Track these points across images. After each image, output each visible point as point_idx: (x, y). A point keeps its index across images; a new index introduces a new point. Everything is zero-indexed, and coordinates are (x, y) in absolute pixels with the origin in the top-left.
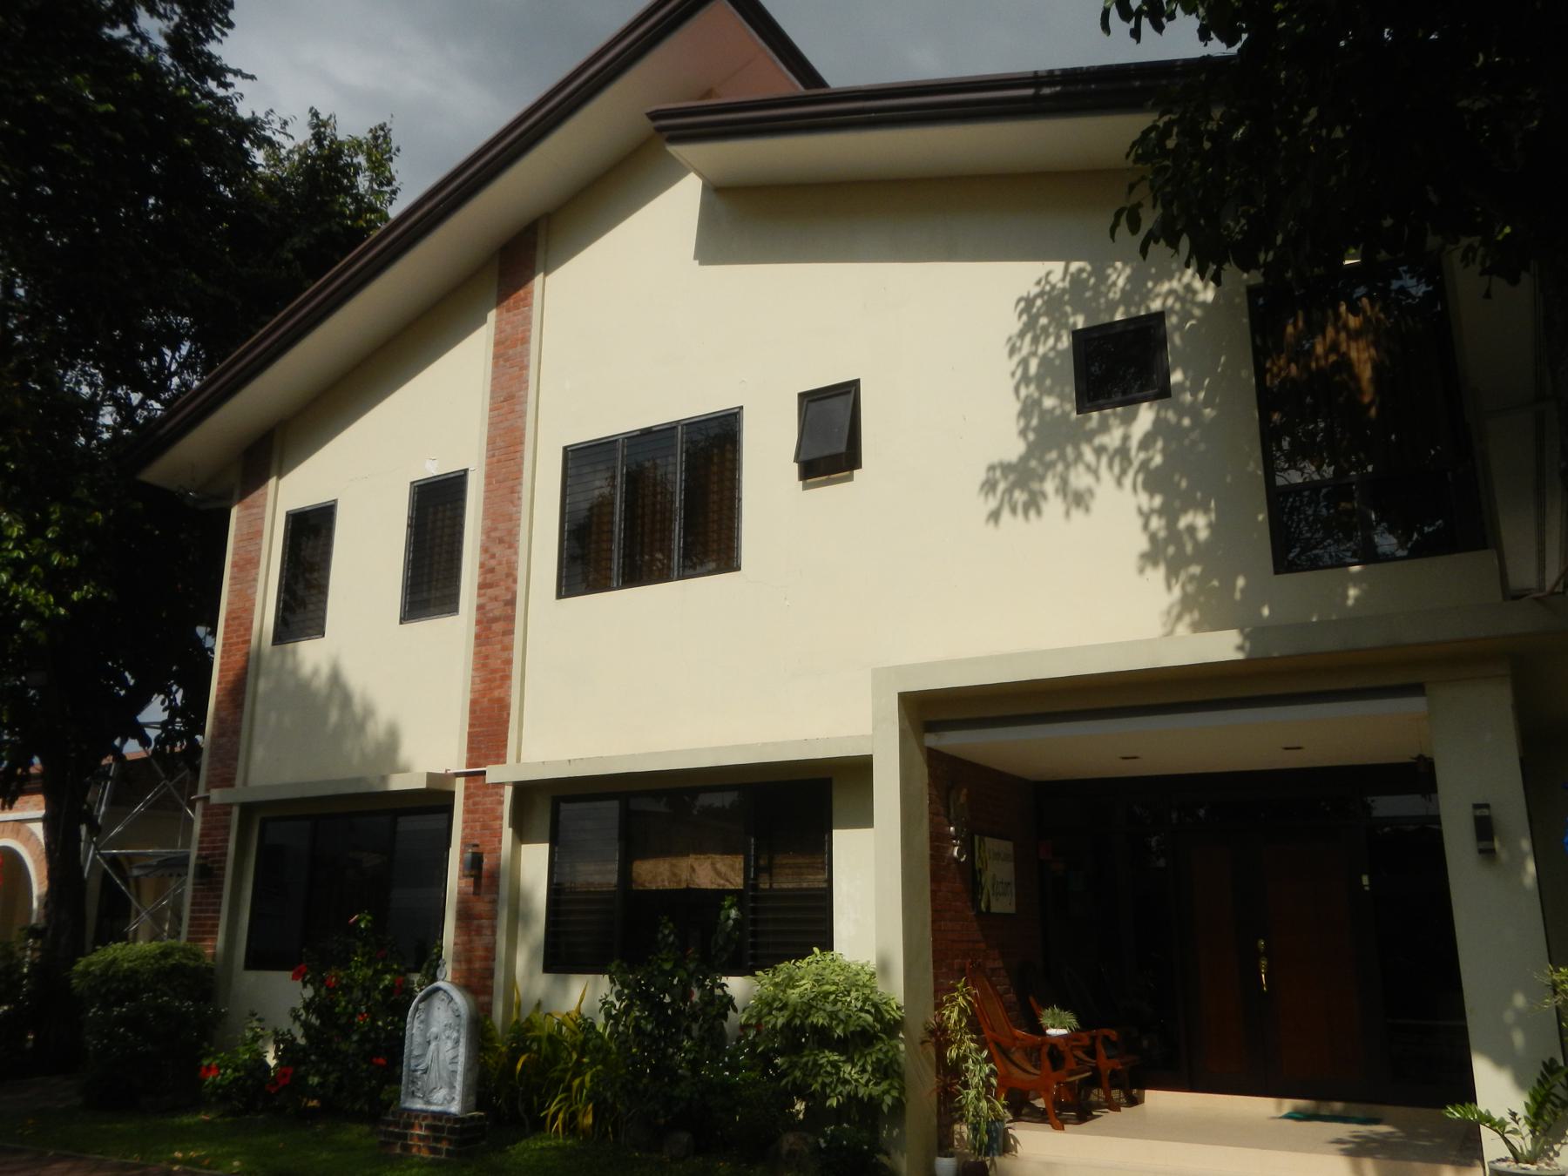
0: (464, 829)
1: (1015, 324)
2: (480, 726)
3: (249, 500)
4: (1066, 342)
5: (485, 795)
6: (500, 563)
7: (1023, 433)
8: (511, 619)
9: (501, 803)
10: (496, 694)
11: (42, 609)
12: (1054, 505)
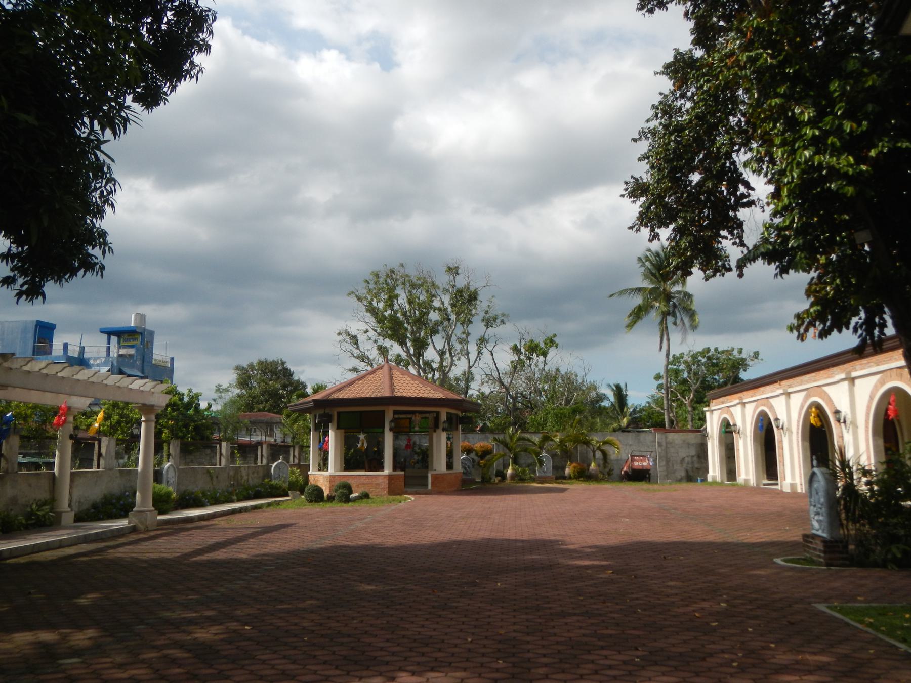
11: (845, 169)
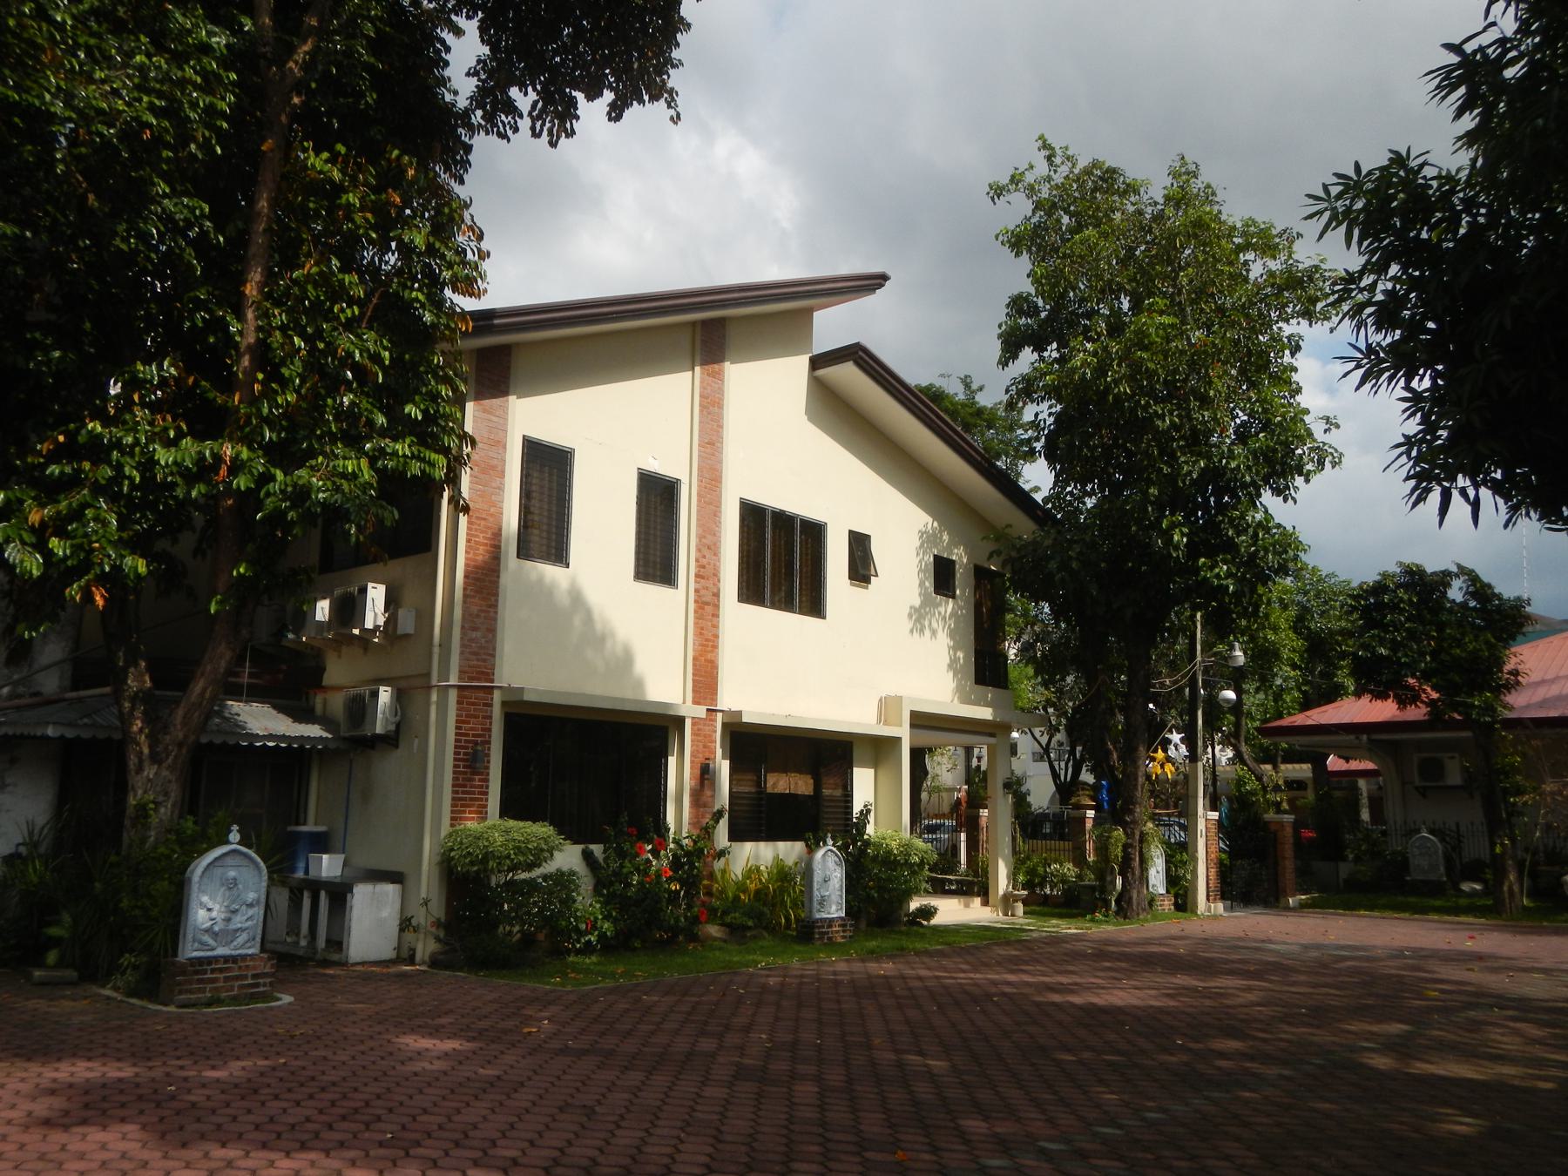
0: (692, 746)
1: (918, 543)
2: (701, 676)
3: (487, 402)
4: (932, 559)
5: (705, 725)
6: (709, 564)
7: (920, 595)
8: (717, 606)
9: (715, 732)
10: (709, 656)
12: (927, 632)
